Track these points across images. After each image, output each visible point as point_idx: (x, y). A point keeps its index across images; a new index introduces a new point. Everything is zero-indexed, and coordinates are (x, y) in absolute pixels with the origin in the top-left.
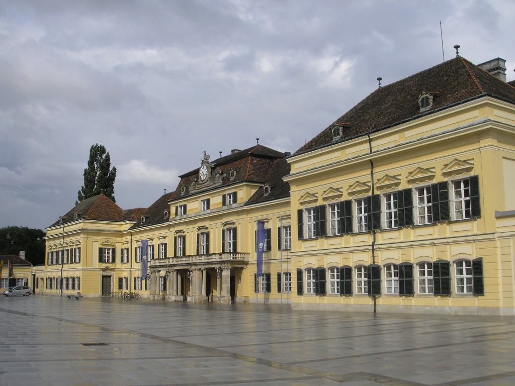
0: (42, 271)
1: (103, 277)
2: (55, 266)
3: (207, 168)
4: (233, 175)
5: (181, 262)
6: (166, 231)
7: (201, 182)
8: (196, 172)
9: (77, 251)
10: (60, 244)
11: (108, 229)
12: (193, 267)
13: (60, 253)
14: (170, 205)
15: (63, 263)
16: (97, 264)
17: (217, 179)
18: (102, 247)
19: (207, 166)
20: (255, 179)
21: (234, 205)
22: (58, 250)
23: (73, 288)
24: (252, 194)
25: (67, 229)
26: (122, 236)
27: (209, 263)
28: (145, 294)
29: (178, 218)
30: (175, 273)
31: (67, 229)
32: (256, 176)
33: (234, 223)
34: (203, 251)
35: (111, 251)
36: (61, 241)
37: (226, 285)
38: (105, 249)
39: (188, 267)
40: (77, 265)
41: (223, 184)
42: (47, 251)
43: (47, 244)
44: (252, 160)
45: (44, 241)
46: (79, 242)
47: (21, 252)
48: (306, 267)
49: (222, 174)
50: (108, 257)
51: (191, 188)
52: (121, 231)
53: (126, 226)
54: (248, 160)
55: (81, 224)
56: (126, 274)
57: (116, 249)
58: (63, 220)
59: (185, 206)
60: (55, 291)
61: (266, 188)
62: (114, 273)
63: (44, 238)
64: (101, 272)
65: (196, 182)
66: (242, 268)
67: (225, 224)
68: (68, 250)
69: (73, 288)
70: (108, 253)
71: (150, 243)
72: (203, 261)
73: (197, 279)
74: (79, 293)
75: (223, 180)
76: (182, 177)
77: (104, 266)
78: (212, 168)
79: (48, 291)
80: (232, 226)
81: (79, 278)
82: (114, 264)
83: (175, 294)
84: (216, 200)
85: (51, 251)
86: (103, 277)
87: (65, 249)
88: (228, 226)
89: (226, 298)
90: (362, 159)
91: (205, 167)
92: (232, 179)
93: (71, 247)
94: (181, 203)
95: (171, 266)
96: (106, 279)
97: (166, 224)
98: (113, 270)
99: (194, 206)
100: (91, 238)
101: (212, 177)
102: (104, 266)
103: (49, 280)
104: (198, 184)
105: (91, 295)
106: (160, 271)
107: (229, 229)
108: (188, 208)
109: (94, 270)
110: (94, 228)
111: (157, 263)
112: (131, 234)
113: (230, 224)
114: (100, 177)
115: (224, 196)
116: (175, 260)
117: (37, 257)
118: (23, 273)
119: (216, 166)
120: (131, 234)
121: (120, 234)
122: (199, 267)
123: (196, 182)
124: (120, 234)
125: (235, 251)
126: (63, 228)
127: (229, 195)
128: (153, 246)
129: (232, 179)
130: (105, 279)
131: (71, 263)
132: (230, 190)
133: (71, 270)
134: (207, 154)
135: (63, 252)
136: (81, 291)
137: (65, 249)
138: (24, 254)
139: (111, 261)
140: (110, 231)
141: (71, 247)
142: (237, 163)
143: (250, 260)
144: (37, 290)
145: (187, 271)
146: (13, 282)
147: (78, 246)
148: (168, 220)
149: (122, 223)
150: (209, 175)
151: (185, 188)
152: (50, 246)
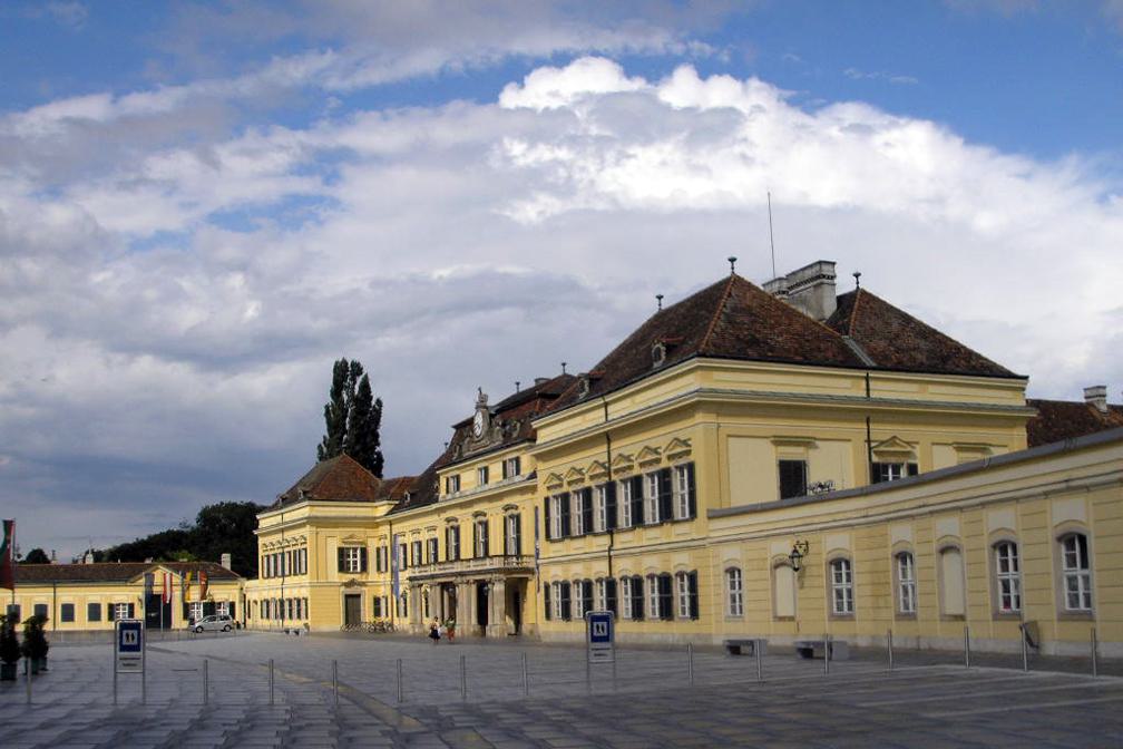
0: (257, 589)
1: (347, 597)
2: (273, 580)
6: (435, 517)
8: (469, 423)
9: (303, 553)
10: (279, 542)
11: (353, 514)
12: (459, 580)
13: (280, 557)
14: (438, 476)
15: (283, 575)
16: (335, 576)
17: (495, 435)
18: (343, 545)
19: (483, 413)
21: (517, 479)
22: (276, 551)
23: (299, 617)
25: (287, 517)
26: (377, 525)
27: (479, 573)
28: (403, 623)
29: (449, 496)
30: (438, 588)
31: (287, 517)
33: (517, 508)
34: (481, 553)
35: (359, 552)
36: (278, 537)
38: (348, 549)
40: (304, 577)
42: (261, 553)
43: (261, 541)
45: (256, 538)
47: (224, 555)
48: (597, 577)
50: (355, 563)
51: (464, 449)
52: (376, 518)
53: (381, 509)
56: (384, 591)
57: (369, 549)
58: (283, 500)
59: (458, 477)
60: (274, 623)
62: (364, 588)
63: (256, 532)
64: (343, 589)
67: (507, 508)
68: (289, 552)
69: (299, 617)
70: (355, 556)
71: (400, 540)
72: (472, 568)
73: (466, 596)
74: (306, 625)
75: (504, 436)
76: (456, 427)
77: (347, 578)
78: (492, 416)
79: (266, 623)
80: (515, 512)
81: (306, 600)
82: (364, 576)
84: (496, 470)
85: (266, 553)
86: (347, 597)
87: (286, 550)
88: (510, 512)
90: (655, 410)
91: (480, 415)
92: (515, 435)
93: (295, 548)
94: (452, 471)
95: (433, 577)
96: (352, 601)
97: (434, 506)
98: (363, 584)
99: (470, 478)
100: (324, 532)
101: (489, 432)
102: (347, 578)
103: (265, 604)
105: (325, 627)
106: (421, 585)
107: (511, 517)
108: (462, 481)
109: (332, 585)
110: (329, 514)
111: (417, 572)
112: (391, 523)
114: (354, 420)
115: (504, 463)
116: (438, 567)
117: (247, 567)
118: (222, 592)
119: (498, 412)
120: (391, 523)
121: (373, 523)
122: (468, 578)
124: (373, 523)
125: (519, 554)
127: (511, 460)
128: (405, 546)
129: (515, 435)
130: (350, 600)
131: (295, 574)
133: (295, 587)
134: (483, 392)
135: (283, 554)
136: (309, 622)
137: (286, 550)
138: (229, 559)
139: (359, 569)
140: (355, 518)
141: (295, 548)
144: (249, 622)
146: (211, 608)
147: (304, 546)
148: (436, 501)
150: (486, 428)
152: (266, 545)
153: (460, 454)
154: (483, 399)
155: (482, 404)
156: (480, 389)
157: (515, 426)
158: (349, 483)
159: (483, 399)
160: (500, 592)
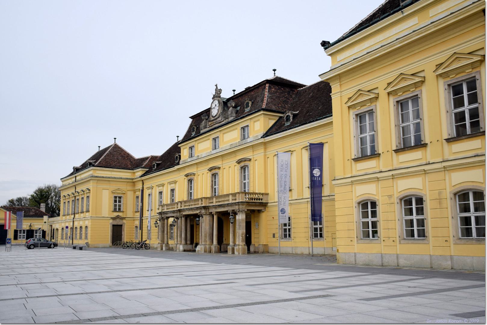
3: (219, 103)
4: (248, 106)
5: (191, 207)
7: (212, 119)
10: (73, 193)
17: (229, 113)
19: (219, 101)
20: (274, 108)
24: (271, 125)
32: (275, 105)
37: (241, 231)
39: (197, 212)
41: (236, 117)
44: (270, 88)
46: (89, 190)
49: (235, 107)
54: (265, 88)
55: (90, 173)
61: (287, 116)
65: (207, 119)
66: (259, 211)
83: (183, 242)
89: (240, 247)
92: (247, 110)
104: (210, 121)
106: (169, 217)
113: (245, 161)
123: (207, 119)
126: (76, 177)
132: (243, 123)
134: (219, 88)
142: (252, 93)
143: (269, 202)
145: (197, 216)
149: (135, 171)
150: (220, 111)
151: (195, 128)
153: (198, 129)
154: (218, 92)
155: (217, 95)
156: (216, 85)
157: (248, 103)
158: (118, 159)
159: (218, 92)
160: (242, 220)
